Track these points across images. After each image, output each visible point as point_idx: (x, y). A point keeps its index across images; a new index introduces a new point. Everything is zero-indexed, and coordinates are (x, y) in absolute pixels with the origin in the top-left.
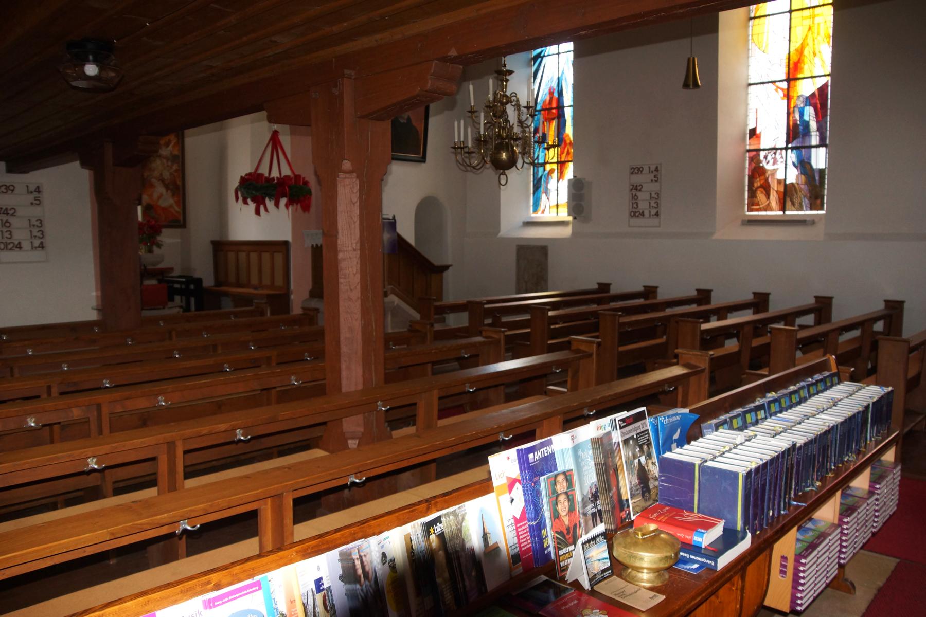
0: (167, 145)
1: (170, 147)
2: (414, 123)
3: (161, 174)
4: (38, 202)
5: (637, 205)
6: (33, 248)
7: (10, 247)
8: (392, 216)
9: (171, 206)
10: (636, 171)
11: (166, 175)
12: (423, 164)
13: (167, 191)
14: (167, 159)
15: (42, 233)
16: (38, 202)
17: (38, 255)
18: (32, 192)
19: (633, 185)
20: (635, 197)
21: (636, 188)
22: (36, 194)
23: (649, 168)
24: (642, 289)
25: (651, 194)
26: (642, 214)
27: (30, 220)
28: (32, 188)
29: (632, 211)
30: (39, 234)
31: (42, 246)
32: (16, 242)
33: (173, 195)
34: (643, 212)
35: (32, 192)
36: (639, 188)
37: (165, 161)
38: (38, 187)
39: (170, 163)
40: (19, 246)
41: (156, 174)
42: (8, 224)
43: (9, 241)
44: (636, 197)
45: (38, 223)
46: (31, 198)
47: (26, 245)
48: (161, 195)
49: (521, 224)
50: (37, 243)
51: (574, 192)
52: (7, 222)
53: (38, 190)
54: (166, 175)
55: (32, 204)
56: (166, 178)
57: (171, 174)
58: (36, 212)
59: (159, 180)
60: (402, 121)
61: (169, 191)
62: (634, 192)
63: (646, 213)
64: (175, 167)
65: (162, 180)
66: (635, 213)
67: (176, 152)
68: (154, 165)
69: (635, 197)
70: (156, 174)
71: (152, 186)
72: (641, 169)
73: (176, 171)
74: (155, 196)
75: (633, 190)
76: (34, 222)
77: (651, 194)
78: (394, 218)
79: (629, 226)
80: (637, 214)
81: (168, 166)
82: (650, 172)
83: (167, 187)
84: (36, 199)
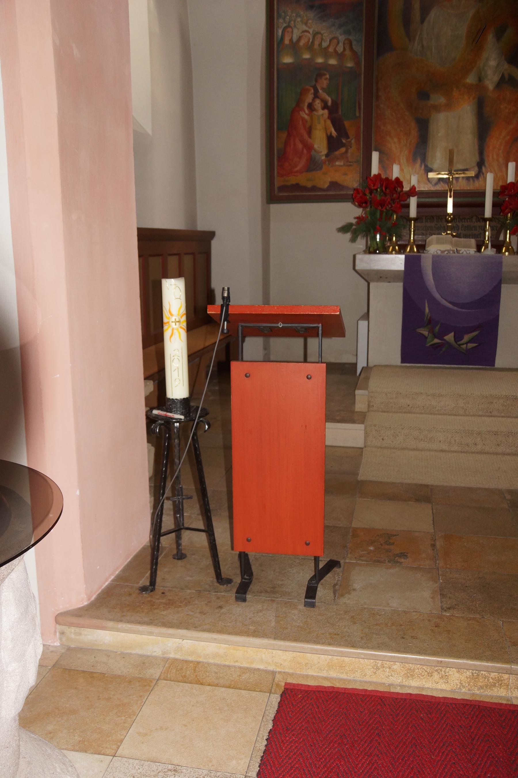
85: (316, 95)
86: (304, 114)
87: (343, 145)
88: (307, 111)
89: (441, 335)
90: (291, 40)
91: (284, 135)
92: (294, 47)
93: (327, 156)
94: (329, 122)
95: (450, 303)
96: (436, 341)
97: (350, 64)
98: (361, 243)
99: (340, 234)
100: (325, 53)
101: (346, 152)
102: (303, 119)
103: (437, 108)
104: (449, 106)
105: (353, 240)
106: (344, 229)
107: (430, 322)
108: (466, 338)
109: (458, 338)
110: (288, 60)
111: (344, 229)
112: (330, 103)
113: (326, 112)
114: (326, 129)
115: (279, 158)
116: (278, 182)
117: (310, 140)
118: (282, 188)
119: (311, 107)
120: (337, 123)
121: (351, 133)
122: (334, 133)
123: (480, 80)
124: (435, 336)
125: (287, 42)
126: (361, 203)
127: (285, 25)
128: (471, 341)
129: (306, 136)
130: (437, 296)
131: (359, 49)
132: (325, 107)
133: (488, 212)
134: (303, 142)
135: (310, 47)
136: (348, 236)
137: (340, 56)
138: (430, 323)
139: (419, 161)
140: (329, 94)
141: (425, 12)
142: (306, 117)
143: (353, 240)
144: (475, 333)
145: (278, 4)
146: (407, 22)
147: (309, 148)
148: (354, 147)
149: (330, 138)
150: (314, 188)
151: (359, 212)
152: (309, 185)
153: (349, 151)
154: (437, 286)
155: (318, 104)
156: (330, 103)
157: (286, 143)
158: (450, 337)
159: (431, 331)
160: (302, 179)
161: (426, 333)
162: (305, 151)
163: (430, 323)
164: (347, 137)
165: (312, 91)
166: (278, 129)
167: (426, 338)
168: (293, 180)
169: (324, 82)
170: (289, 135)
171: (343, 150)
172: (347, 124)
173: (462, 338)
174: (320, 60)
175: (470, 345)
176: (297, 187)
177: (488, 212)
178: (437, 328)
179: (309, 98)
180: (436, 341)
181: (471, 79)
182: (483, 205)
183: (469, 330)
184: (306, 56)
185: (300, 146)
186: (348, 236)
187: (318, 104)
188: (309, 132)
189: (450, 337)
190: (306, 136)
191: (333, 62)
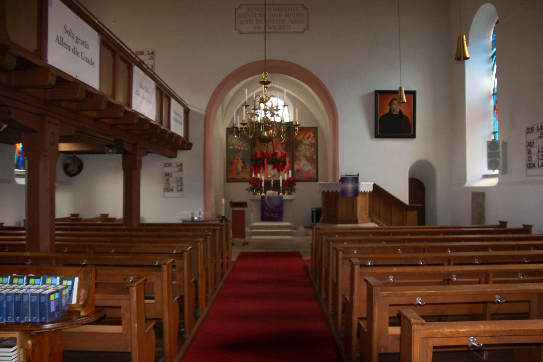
0: (308, 138)
1: (310, 139)
2: (404, 113)
3: (305, 154)
4: (181, 170)
5: (531, 159)
6: (178, 191)
7: (169, 190)
8: (357, 173)
9: (310, 170)
10: (530, 131)
11: (308, 154)
12: (415, 139)
13: (308, 162)
14: (309, 146)
15: (182, 184)
17: (178, 194)
18: (179, 166)
19: (529, 143)
20: (529, 152)
21: (530, 144)
22: (180, 167)
23: (537, 127)
24: (522, 227)
25: (538, 148)
26: (534, 166)
28: (179, 164)
29: (528, 164)
30: (180, 185)
31: (181, 190)
32: (171, 188)
33: (311, 165)
34: (535, 164)
36: (532, 144)
37: (307, 147)
39: (310, 148)
40: (172, 190)
41: (302, 153)
42: (168, 180)
43: (168, 187)
44: (530, 152)
45: (180, 180)
47: (175, 189)
48: (305, 165)
49: (481, 177)
50: (179, 189)
51: (490, 151)
52: (168, 179)
53: (181, 165)
54: (308, 154)
55: (178, 171)
56: (307, 155)
57: (310, 153)
59: (304, 157)
60: (395, 113)
61: (309, 162)
62: (529, 148)
63: (536, 165)
64: (313, 149)
65: (305, 157)
66: (530, 164)
67: (313, 141)
68: (301, 149)
69: (529, 152)
70: (302, 153)
71: (300, 160)
72: (533, 129)
73: (313, 151)
74: (301, 165)
75: (529, 147)
76: (179, 179)
77: (538, 148)
78: (358, 175)
79: (527, 176)
80: (531, 166)
81: (309, 149)
82: (538, 130)
83: (308, 160)
84: (180, 169)
85: (239, 156)
86: (236, 161)
92: (233, 145)
93: (242, 171)
96: (269, 216)
97: (247, 149)
98: (251, 192)
100: (240, 146)
108: (276, 214)
109: (274, 215)
110: (231, 147)
111: (247, 189)
113: (241, 160)
116: (229, 177)
119: (237, 159)
120: (244, 163)
122: (243, 165)
125: (231, 143)
126: (251, 183)
127: (230, 139)
130: (269, 206)
131: (250, 146)
132: (241, 159)
133: (281, 185)
135: (237, 145)
137: (245, 147)
143: (249, 192)
147: (237, 169)
150: (239, 179)
151: (251, 186)
156: (242, 157)
158: (272, 215)
161: (266, 213)
168: (233, 177)
169: (241, 153)
174: (239, 148)
175: (277, 216)
176: (234, 178)
177: (281, 185)
179: (237, 157)
182: (279, 183)
184: (236, 147)
185: (234, 168)
186: (247, 191)
187: (239, 158)
188: (237, 165)
191: (243, 148)
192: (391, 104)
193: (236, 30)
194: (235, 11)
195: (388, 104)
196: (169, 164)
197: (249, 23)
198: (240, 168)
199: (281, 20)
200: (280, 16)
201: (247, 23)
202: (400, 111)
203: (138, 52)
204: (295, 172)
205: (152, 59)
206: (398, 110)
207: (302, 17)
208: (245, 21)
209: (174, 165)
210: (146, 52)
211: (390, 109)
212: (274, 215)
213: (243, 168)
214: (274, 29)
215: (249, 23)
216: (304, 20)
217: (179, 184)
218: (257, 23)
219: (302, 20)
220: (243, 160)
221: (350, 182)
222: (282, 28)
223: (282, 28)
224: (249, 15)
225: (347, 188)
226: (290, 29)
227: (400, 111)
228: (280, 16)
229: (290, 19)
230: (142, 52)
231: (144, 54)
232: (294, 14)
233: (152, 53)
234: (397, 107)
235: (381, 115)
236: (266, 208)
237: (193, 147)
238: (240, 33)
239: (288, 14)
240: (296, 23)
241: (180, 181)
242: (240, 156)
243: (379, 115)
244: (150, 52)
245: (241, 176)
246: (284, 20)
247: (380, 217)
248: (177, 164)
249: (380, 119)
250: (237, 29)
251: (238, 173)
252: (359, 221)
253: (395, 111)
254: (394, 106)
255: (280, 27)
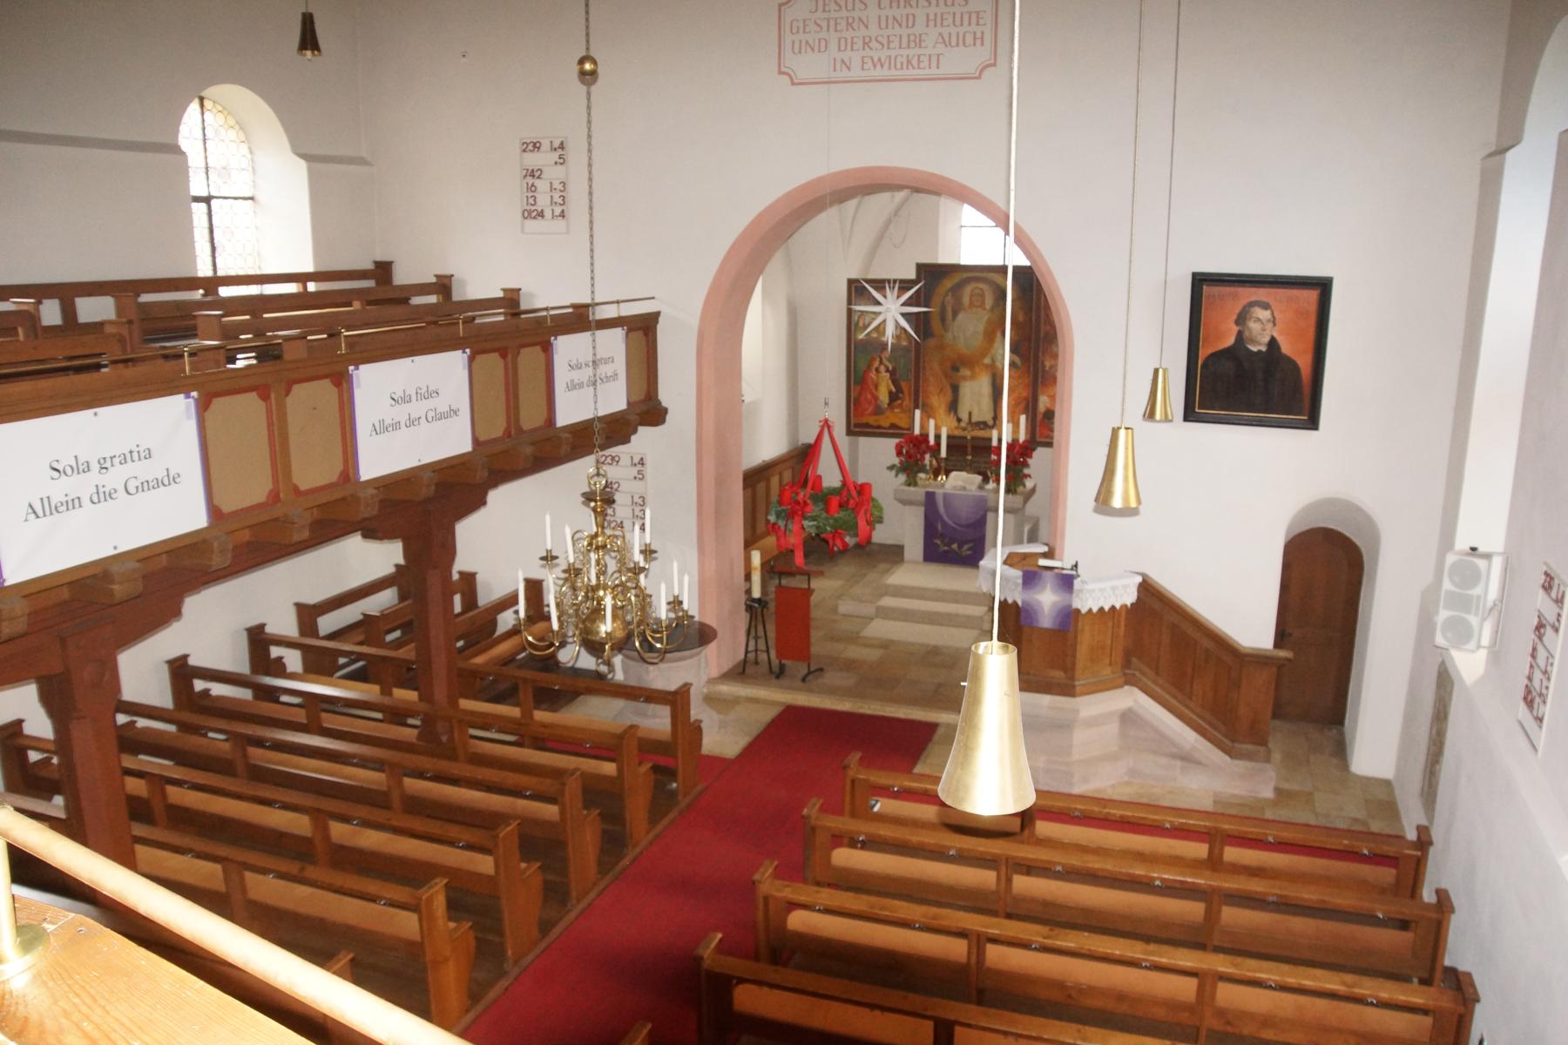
2: (1286, 348)
4: (641, 477)
16: (641, 476)
18: (635, 465)
22: (639, 467)
27: (632, 497)
32: (619, 522)
35: (635, 465)
38: (642, 459)
45: (640, 501)
46: (634, 471)
53: (642, 462)
58: (637, 487)
60: (1254, 349)
76: (636, 499)
85: (881, 362)
86: (873, 375)
87: (900, 398)
88: (874, 372)
89: (949, 545)
90: (864, 324)
91: (859, 388)
94: (890, 382)
95: (955, 523)
96: (946, 548)
99: (888, 472)
101: (902, 403)
102: (871, 377)
103: (965, 378)
104: (973, 377)
105: (897, 475)
106: (891, 468)
107: (941, 535)
108: (966, 547)
109: (960, 547)
111: (891, 468)
112: (890, 368)
113: (888, 375)
114: (888, 386)
115: (855, 405)
117: (875, 393)
118: (856, 425)
120: (895, 382)
121: (905, 390)
122: (894, 390)
123: (993, 361)
124: (945, 545)
125: (861, 324)
128: (969, 549)
129: (874, 390)
130: (945, 518)
132: (887, 371)
134: (872, 394)
136: (894, 472)
138: (942, 536)
139: (952, 414)
140: (890, 362)
141: (955, 314)
142: (873, 376)
143: (897, 475)
144: (970, 545)
145: (855, 298)
146: (943, 319)
147: (876, 398)
148: (907, 397)
149: (890, 393)
150: (879, 427)
152: (875, 424)
153: (904, 403)
154: (947, 512)
155: (882, 368)
156: (890, 368)
157: (860, 394)
158: (955, 546)
159: (942, 541)
160: (872, 420)
161: (938, 542)
162: (873, 401)
163: (942, 536)
164: (902, 393)
165: (878, 359)
166: (854, 383)
167: (938, 546)
168: (864, 420)
170: (862, 388)
171: (899, 402)
172: (903, 384)
173: (962, 547)
175: (968, 552)
176: (867, 425)
178: (946, 540)
179: (876, 364)
180: (946, 548)
181: (987, 361)
183: (967, 542)
185: (869, 396)
186: (894, 472)
187: (882, 368)
188: (876, 387)
189: (955, 546)
190: (874, 390)
192: (1242, 319)
193: (780, 73)
194: (780, 11)
195: (1235, 317)
196: (613, 458)
197: (816, 49)
198: (884, 397)
199: (912, 38)
200: (910, 24)
201: (813, 49)
202: (1273, 343)
203: (528, 144)
204: (1039, 417)
205: (561, 164)
206: (1267, 339)
207: (978, 24)
208: (807, 42)
209: (625, 460)
210: (546, 145)
211: (1240, 334)
212: (960, 547)
213: (893, 397)
214: (890, 68)
215: (816, 49)
216: (983, 33)
217: (637, 509)
218: (839, 50)
219: (979, 35)
220: (893, 373)
221: (1049, 587)
222: (915, 62)
223: (915, 62)
224: (819, 25)
225: (1040, 602)
226: (938, 68)
227: (1273, 343)
228: (910, 24)
229: (941, 34)
230: (538, 142)
231: (542, 148)
232: (954, 14)
233: (562, 146)
234: (1264, 330)
235: (1211, 351)
236: (940, 527)
237: (669, 417)
238: (793, 83)
239: (936, 15)
240: (958, 45)
241: (640, 505)
242: (884, 360)
243: (1203, 353)
244: (556, 144)
245: (885, 422)
246: (920, 35)
247: (1157, 674)
248: (632, 458)
249: (1204, 365)
250: (783, 69)
251: (878, 411)
252: (1078, 689)
253: (1254, 342)
254: (1253, 326)
255: (909, 62)
